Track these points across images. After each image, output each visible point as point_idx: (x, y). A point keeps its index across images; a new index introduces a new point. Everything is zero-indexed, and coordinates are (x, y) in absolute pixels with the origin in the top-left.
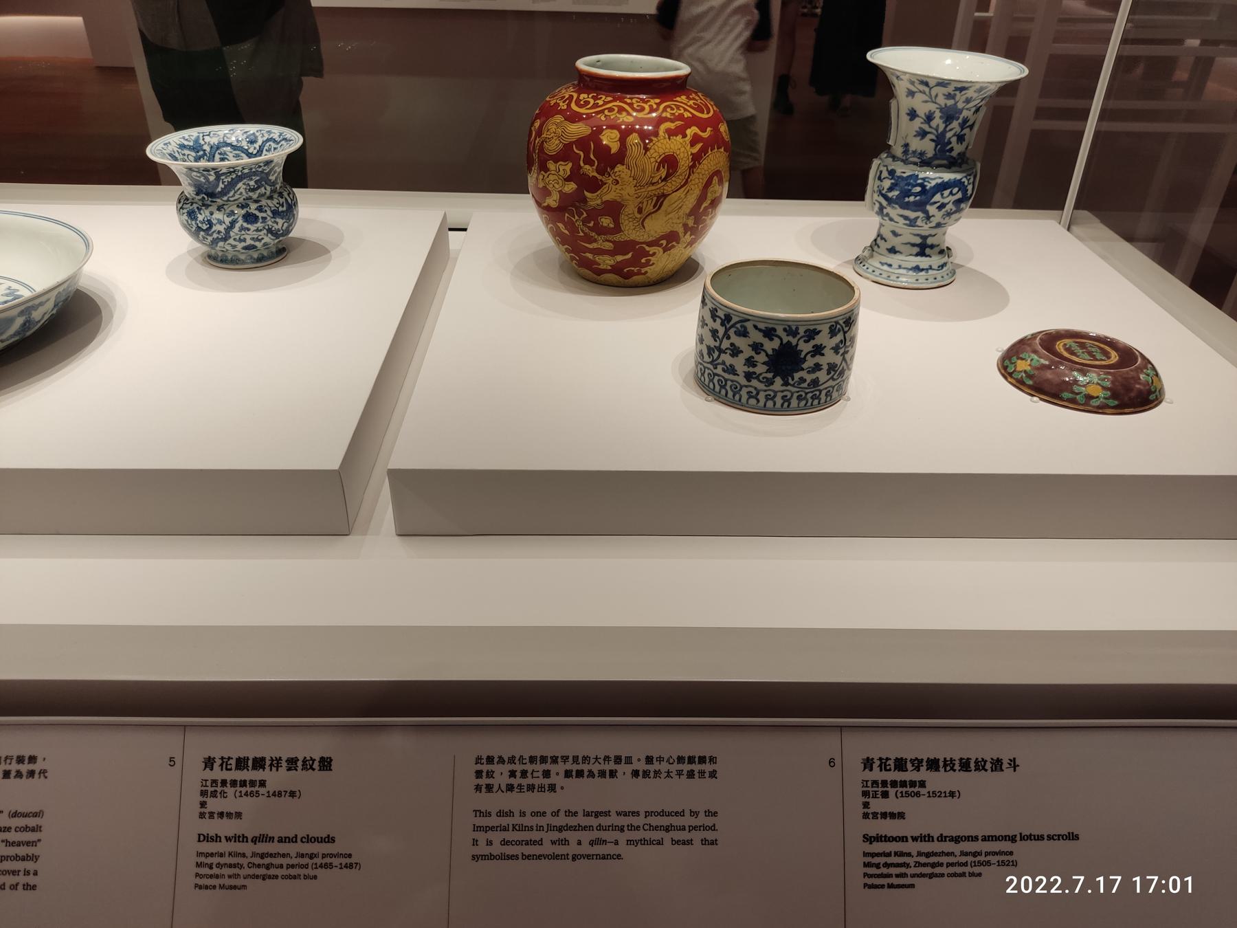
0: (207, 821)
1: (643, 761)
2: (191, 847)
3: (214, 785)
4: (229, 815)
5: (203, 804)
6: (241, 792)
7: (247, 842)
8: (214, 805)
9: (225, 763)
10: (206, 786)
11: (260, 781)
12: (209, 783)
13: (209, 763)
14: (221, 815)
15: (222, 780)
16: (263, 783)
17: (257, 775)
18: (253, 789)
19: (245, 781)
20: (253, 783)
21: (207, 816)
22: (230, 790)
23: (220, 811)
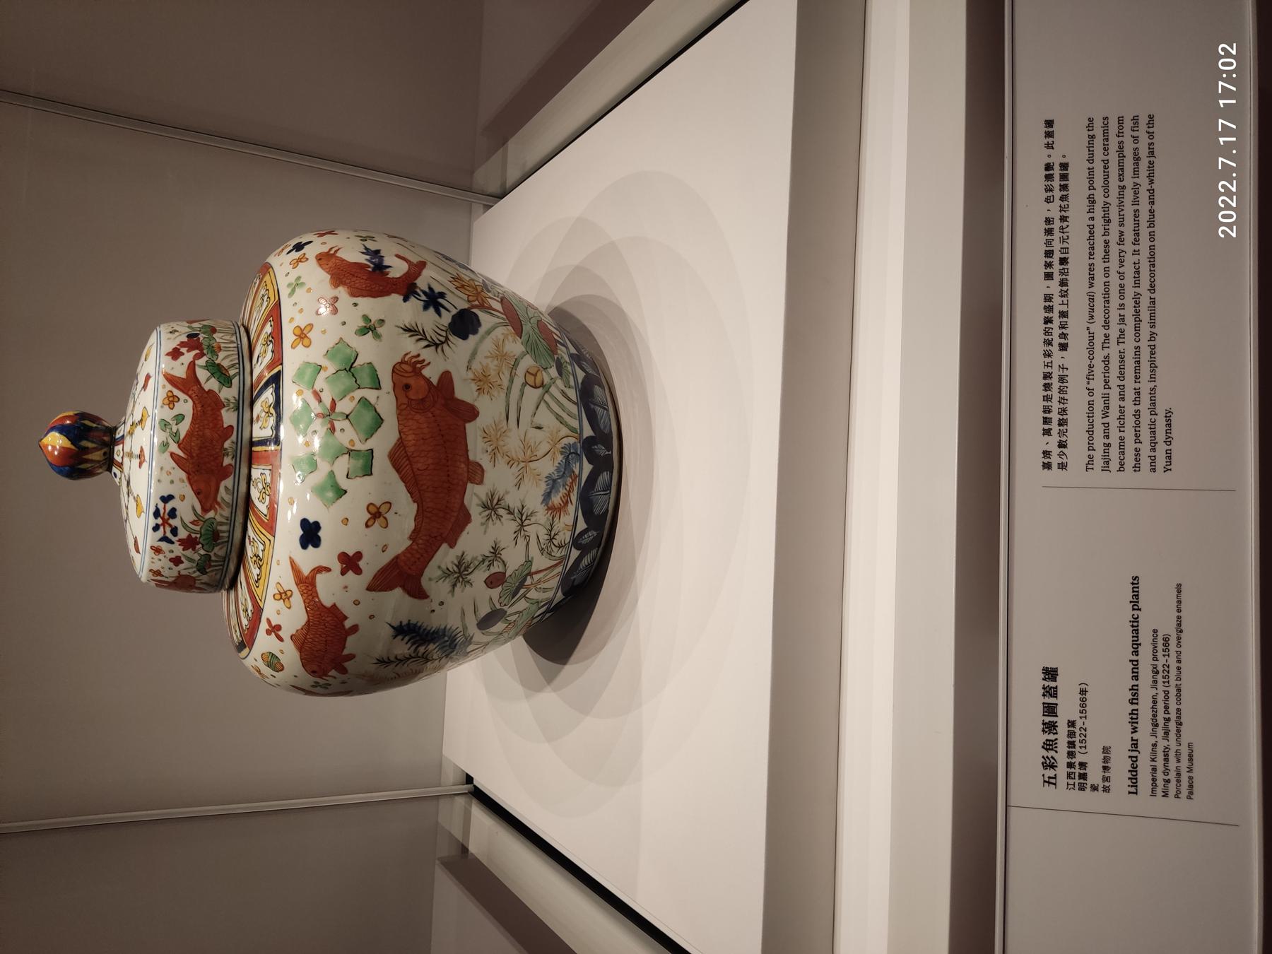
0: (1112, 784)
1: (1049, 282)
2: (1144, 801)
3: (1073, 776)
4: (1106, 760)
5: (1094, 788)
6: (1080, 747)
7: (1137, 686)
8: (1095, 776)
9: (1049, 764)
10: (1074, 785)
12: (1071, 782)
13: (1050, 781)
14: (1105, 769)
15: (1068, 767)
16: (1072, 724)
17: (1063, 729)
18: (1077, 735)
19: (1069, 742)
20: (1071, 734)
21: (1107, 784)
22: (1079, 758)
23: (1102, 770)
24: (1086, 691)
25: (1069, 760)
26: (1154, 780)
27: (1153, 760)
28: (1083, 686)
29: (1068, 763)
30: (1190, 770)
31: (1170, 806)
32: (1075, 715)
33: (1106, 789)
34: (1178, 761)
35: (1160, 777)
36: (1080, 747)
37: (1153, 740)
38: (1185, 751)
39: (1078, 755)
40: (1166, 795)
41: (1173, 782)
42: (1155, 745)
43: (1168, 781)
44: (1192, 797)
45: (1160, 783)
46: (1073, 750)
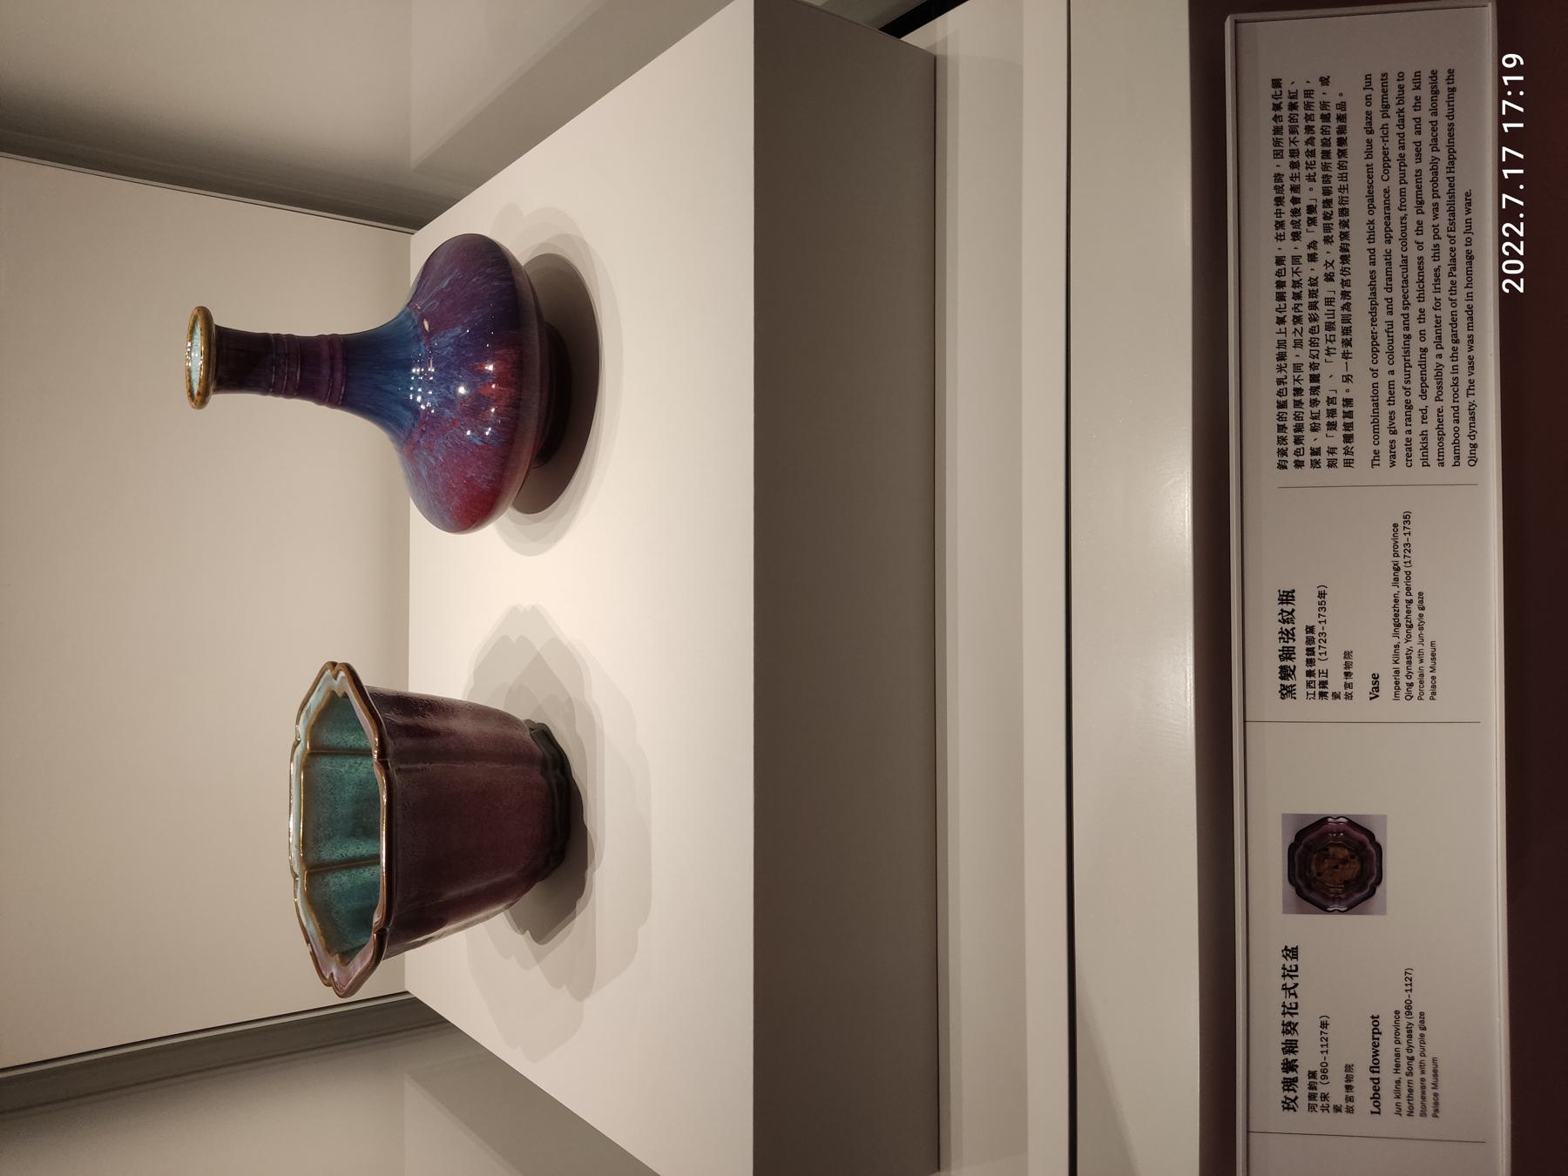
0: (1355, 691)
3: (1312, 685)
4: (1348, 666)
5: (1336, 696)
6: (1320, 654)
8: (1336, 683)
9: (1285, 673)
10: (1314, 694)
11: (1307, 632)
12: (1311, 691)
13: (1287, 692)
14: (1347, 675)
16: (1310, 629)
17: (1301, 636)
18: (1316, 641)
19: (1308, 650)
20: (1310, 641)
21: (1349, 691)
22: (1319, 666)
23: (1343, 676)
24: (1325, 594)
25: (1309, 668)
26: (1397, 683)
27: (1396, 662)
28: (1322, 589)
29: (1307, 671)
30: (1433, 669)
31: (1414, 709)
32: (1313, 621)
33: (1349, 696)
34: (1421, 661)
35: (1403, 681)
36: (1320, 654)
37: (1396, 641)
38: (1428, 651)
39: (1317, 662)
40: (1409, 697)
41: (1417, 684)
42: (1397, 646)
43: (1411, 685)
44: (1435, 697)
45: (1403, 686)
46: (1313, 657)
